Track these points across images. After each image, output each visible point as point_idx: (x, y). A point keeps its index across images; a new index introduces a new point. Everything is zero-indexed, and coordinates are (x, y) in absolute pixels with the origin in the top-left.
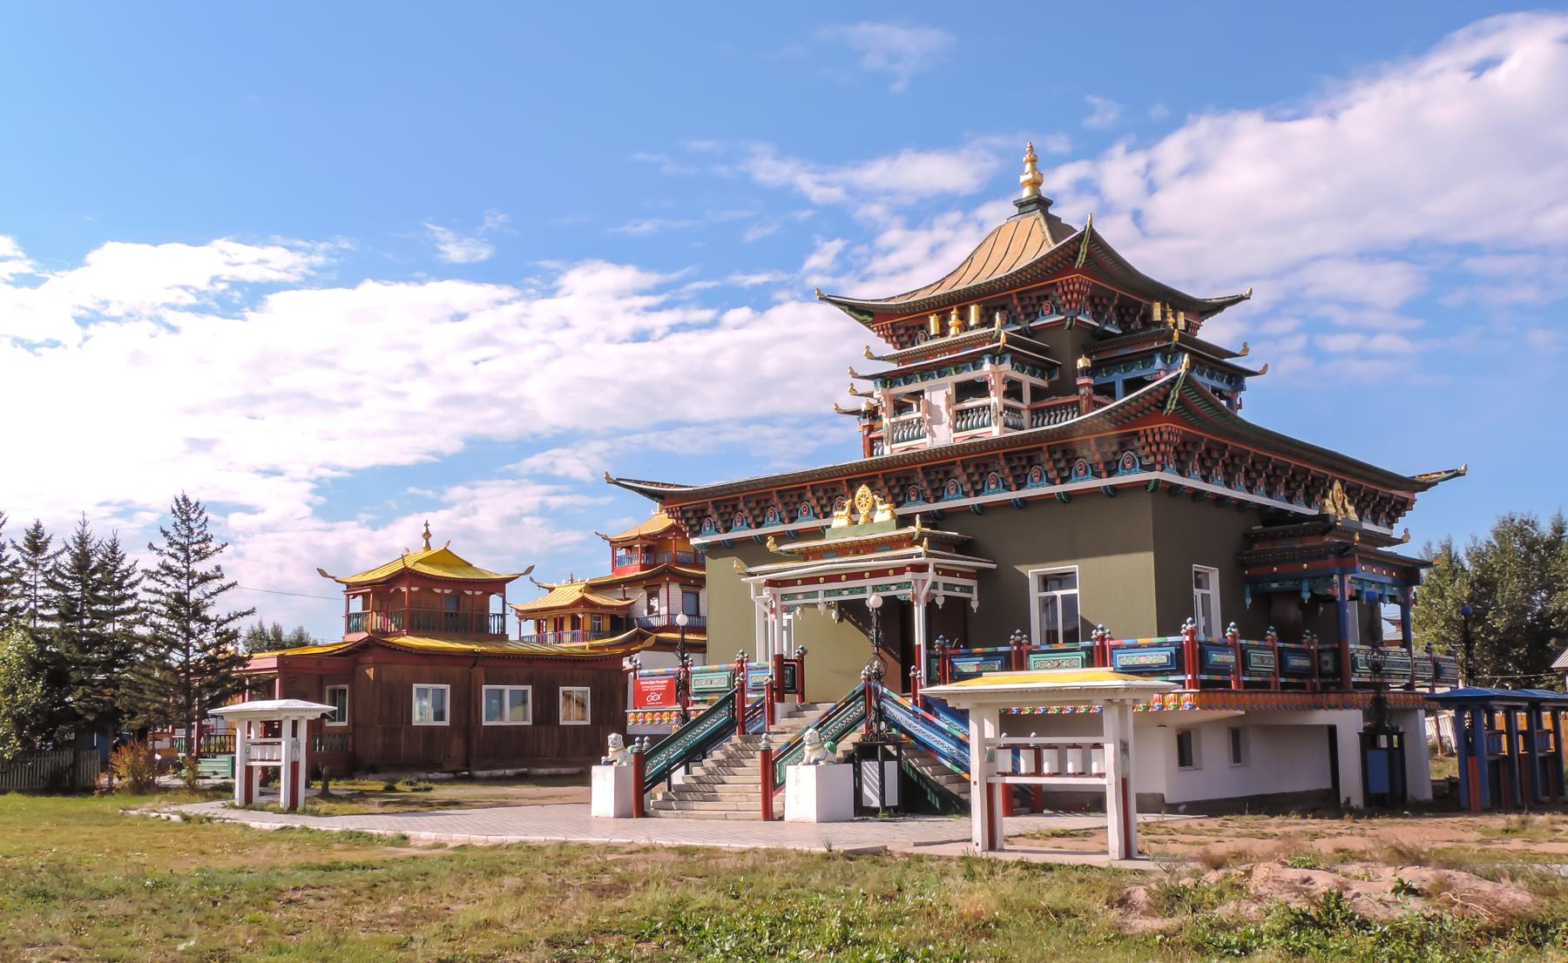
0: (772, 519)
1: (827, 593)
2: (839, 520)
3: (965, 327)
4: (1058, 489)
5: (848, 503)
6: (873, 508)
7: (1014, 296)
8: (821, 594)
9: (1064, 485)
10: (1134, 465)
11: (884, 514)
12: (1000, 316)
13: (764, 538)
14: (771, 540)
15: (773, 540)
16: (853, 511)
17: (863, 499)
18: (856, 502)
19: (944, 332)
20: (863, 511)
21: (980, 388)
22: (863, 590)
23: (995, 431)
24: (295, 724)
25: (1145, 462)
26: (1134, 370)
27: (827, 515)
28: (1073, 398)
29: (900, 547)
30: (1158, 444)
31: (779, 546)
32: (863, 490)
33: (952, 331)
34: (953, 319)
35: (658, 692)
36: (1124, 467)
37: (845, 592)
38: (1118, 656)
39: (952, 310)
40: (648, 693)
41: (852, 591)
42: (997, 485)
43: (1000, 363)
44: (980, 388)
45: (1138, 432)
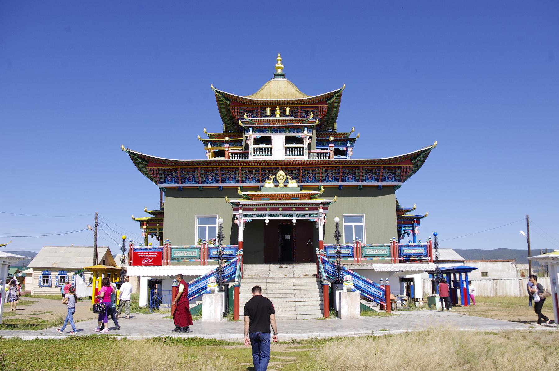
0: (210, 180)
4: (360, 183)
6: (286, 181)
9: (302, 183)
10: (392, 179)
11: (293, 184)
13: (237, 188)
14: (239, 188)
16: (276, 181)
18: (277, 177)
19: (273, 114)
20: (281, 182)
21: (301, 141)
23: (305, 158)
25: (396, 178)
27: (263, 182)
29: (305, 199)
32: (281, 173)
33: (278, 116)
34: (278, 112)
35: (151, 258)
36: (388, 179)
39: (277, 107)
40: (144, 258)
42: (332, 179)
45: (401, 166)
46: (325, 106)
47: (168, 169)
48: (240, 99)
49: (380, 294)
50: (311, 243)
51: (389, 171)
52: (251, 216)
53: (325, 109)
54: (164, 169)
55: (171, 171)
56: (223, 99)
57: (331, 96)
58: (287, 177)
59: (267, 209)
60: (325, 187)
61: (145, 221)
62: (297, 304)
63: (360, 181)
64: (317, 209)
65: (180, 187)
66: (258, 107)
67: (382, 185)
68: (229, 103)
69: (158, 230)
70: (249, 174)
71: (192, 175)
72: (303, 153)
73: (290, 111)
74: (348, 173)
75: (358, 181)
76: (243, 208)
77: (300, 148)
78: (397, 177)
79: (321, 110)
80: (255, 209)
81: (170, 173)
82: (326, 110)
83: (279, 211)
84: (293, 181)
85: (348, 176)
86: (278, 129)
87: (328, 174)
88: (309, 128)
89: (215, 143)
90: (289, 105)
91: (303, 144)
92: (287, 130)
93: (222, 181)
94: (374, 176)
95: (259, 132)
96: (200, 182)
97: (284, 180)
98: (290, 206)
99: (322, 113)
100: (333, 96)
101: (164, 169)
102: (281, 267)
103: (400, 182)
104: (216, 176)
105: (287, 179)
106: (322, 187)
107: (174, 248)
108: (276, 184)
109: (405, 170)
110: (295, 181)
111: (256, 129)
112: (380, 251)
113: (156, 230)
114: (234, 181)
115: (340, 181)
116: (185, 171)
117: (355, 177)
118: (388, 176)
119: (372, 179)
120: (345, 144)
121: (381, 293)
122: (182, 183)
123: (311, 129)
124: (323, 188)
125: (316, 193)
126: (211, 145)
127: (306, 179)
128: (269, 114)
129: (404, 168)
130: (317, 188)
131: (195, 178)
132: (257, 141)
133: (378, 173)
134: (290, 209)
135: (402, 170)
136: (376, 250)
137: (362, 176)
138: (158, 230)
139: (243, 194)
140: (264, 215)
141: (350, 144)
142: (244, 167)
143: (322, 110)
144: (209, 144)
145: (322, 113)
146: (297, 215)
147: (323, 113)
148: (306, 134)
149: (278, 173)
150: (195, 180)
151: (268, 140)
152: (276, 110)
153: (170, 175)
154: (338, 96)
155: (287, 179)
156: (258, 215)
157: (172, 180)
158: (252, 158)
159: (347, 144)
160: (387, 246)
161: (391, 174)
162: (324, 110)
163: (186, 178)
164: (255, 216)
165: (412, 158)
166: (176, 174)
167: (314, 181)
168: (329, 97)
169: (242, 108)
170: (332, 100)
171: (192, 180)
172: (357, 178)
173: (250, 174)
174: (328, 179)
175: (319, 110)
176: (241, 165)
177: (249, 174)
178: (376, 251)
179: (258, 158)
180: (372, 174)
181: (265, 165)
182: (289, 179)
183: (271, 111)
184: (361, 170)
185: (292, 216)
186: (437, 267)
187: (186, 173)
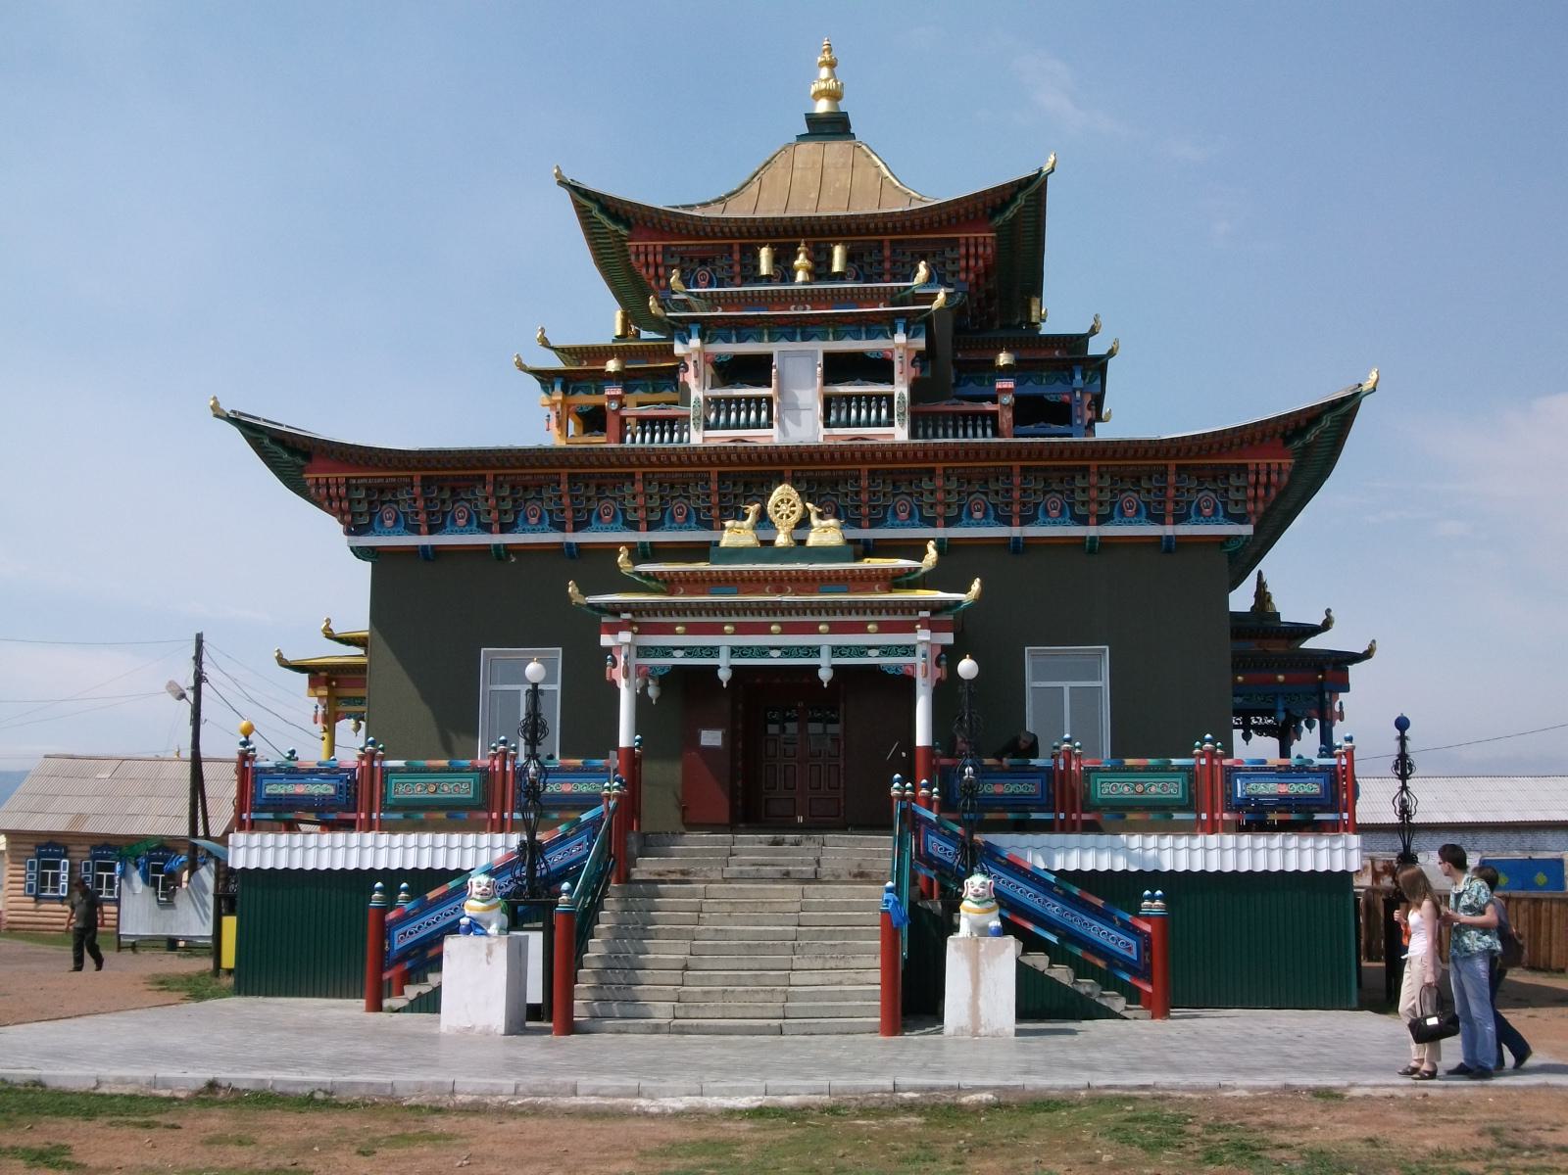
1: (735, 651)
2: (737, 534)
4: (1092, 531)
5: (752, 509)
6: (804, 523)
7: (887, 244)
8: (724, 653)
10: (1215, 511)
11: (826, 533)
12: (926, 267)
13: (612, 549)
15: (627, 553)
17: (783, 507)
19: (784, 269)
21: (880, 369)
22: (815, 651)
23: (900, 433)
25: (1232, 509)
26: (1030, 384)
28: (988, 406)
30: (1267, 486)
31: (635, 564)
33: (800, 276)
36: (1199, 511)
37: (775, 653)
38: (1099, 780)
41: (787, 651)
42: (986, 515)
43: (913, 337)
44: (880, 369)
45: (1246, 465)
46: (985, 238)
47: (379, 481)
48: (663, 217)
49: (1130, 949)
50: (904, 754)
51: (1200, 483)
52: (666, 652)
53: (985, 247)
54: (365, 481)
55: (394, 488)
56: (601, 217)
57: (1007, 198)
58: (805, 507)
59: (821, 627)
60: (940, 546)
61: (326, 671)
62: (796, 978)
63: (1092, 519)
64: (909, 628)
65: (425, 547)
66: (731, 246)
67: (1101, 537)
68: (625, 232)
70: (673, 498)
71: (469, 501)
72: (890, 414)
73: (849, 258)
74: (1045, 493)
75: (1083, 521)
76: (637, 624)
77: (879, 397)
78: (1234, 507)
79: (968, 250)
81: (390, 496)
82: (989, 250)
83: (675, 633)
84: (824, 523)
85: (970, 505)
86: (796, 327)
87: (969, 494)
88: (914, 323)
89: (579, 380)
90: (769, 236)
91: (892, 383)
92: (831, 330)
93: (575, 524)
94: (1147, 504)
95: (727, 340)
96: (496, 527)
97: (794, 518)
98: (809, 618)
99: (972, 262)
100: (1013, 198)
101: (365, 481)
102: (776, 843)
103: (1247, 523)
104: (553, 507)
105: (806, 512)
106: (931, 546)
107: (395, 770)
108: (766, 535)
109: (1263, 479)
110: (832, 522)
111: (710, 330)
112: (1153, 789)
114: (474, 527)
115: (1016, 520)
116: (441, 489)
117: (1072, 506)
118: (1199, 503)
119: (1138, 512)
120: (1065, 377)
121: (1133, 943)
122: (432, 530)
123: (923, 326)
124: (935, 548)
125: (910, 569)
126: (565, 390)
127: (885, 513)
128: (765, 268)
129: (1257, 474)
130: (916, 550)
131: (478, 513)
132: (731, 371)
133: (1160, 491)
134: (812, 629)
135: (1252, 478)
136: (1136, 783)
137: (1101, 504)
139: (639, 573)
140: (713, 651)
141: (1084, 378)
142: (653, 473)
143: (972, 250)
144: (558, 388)
145: (972, 262)
146: (837, 651)
147: (976, 263)
148: (900, 344)
149: (775, 494)
150: (478, 518)
151: (757, 369)
152: (796, 257)
153: (390, 501)
154: (1032, 198)
155: (806, 512)
156: (690, 651)
157: (396, 521)
158: (696, 437)
159: (1072, 377)
160: (1181, 768)
161: (1213, 495)
162: (981, 250)
163: (445, 514)
164: (680, 653)
165: (1288, 433)
166: (410, 499)
167: (693, 525)
168: (999, 201)
169: (674, 249)
170: (1009, 214)
172: (1080, 510)
173: (680, 495)
174: (970, 515)
175: (963, 250)
176: (641, 465)
177: (677, 497)
178: (1139, 788)
179: (720, 437)
180: (1136, 495)
181: (731, 463)
182: (813, 516)
183: (776, 260)
184: (1094, 479)
185: (818, 652)
186: (1407, 848)
187: (446, 495)
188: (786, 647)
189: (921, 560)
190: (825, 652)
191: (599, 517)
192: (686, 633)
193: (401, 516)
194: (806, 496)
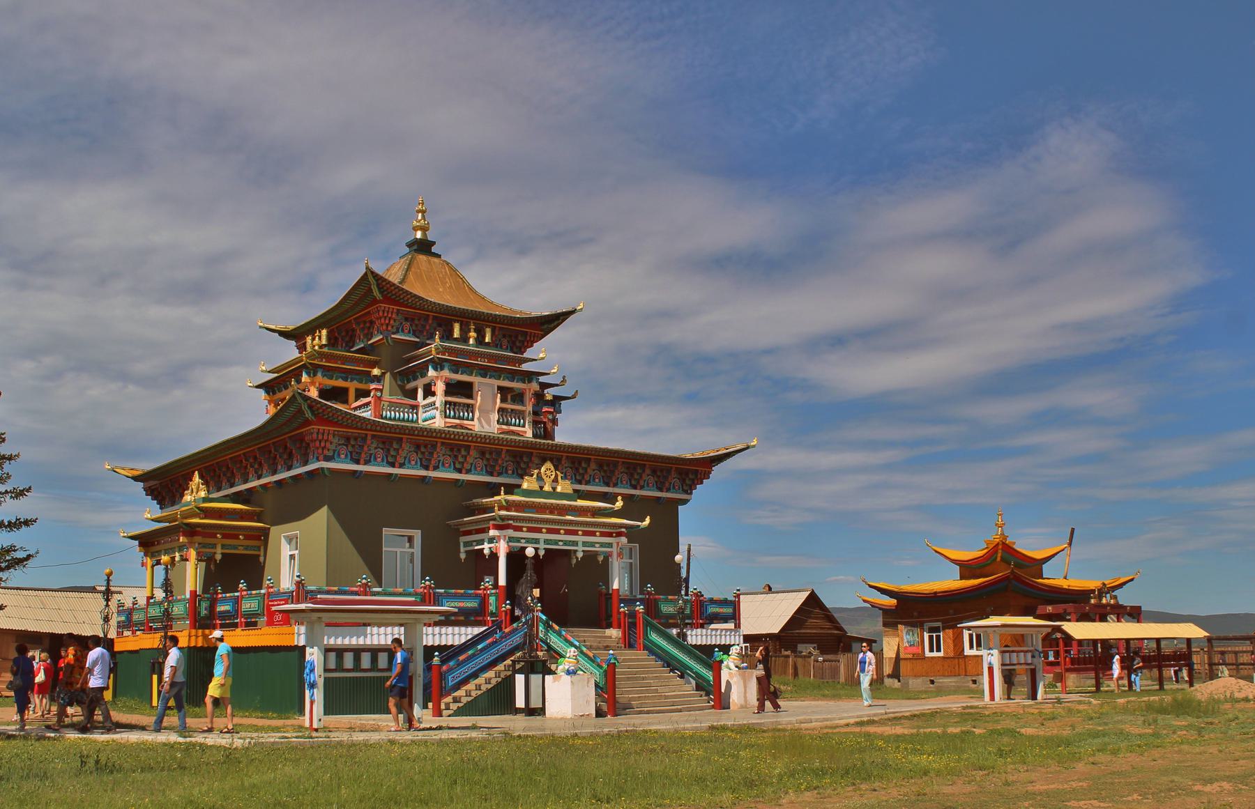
1: (547, 542)
3: (480, 341)
6: (555, 480)
11: (564, 486)
16: (539, 478)
22: (575, 543)
24: (1032, 635)
27: (522, 477)
29: (586, 516)
37: (561, 543)
41: (566, 543)
69: (219, 547)
80: (524, 529)
113: (214, 546)
128: (456, 334)
130: (610, 498)
138: (219, 547)
151: (465, 389)
155: (556, 475)
171: (383, 460)
188: (565, 541)
189: (614, 505)
190: (580, 544)
191: (443, 465)
192: (547, 533)
193: (349, 453)
194: (556, 468)
